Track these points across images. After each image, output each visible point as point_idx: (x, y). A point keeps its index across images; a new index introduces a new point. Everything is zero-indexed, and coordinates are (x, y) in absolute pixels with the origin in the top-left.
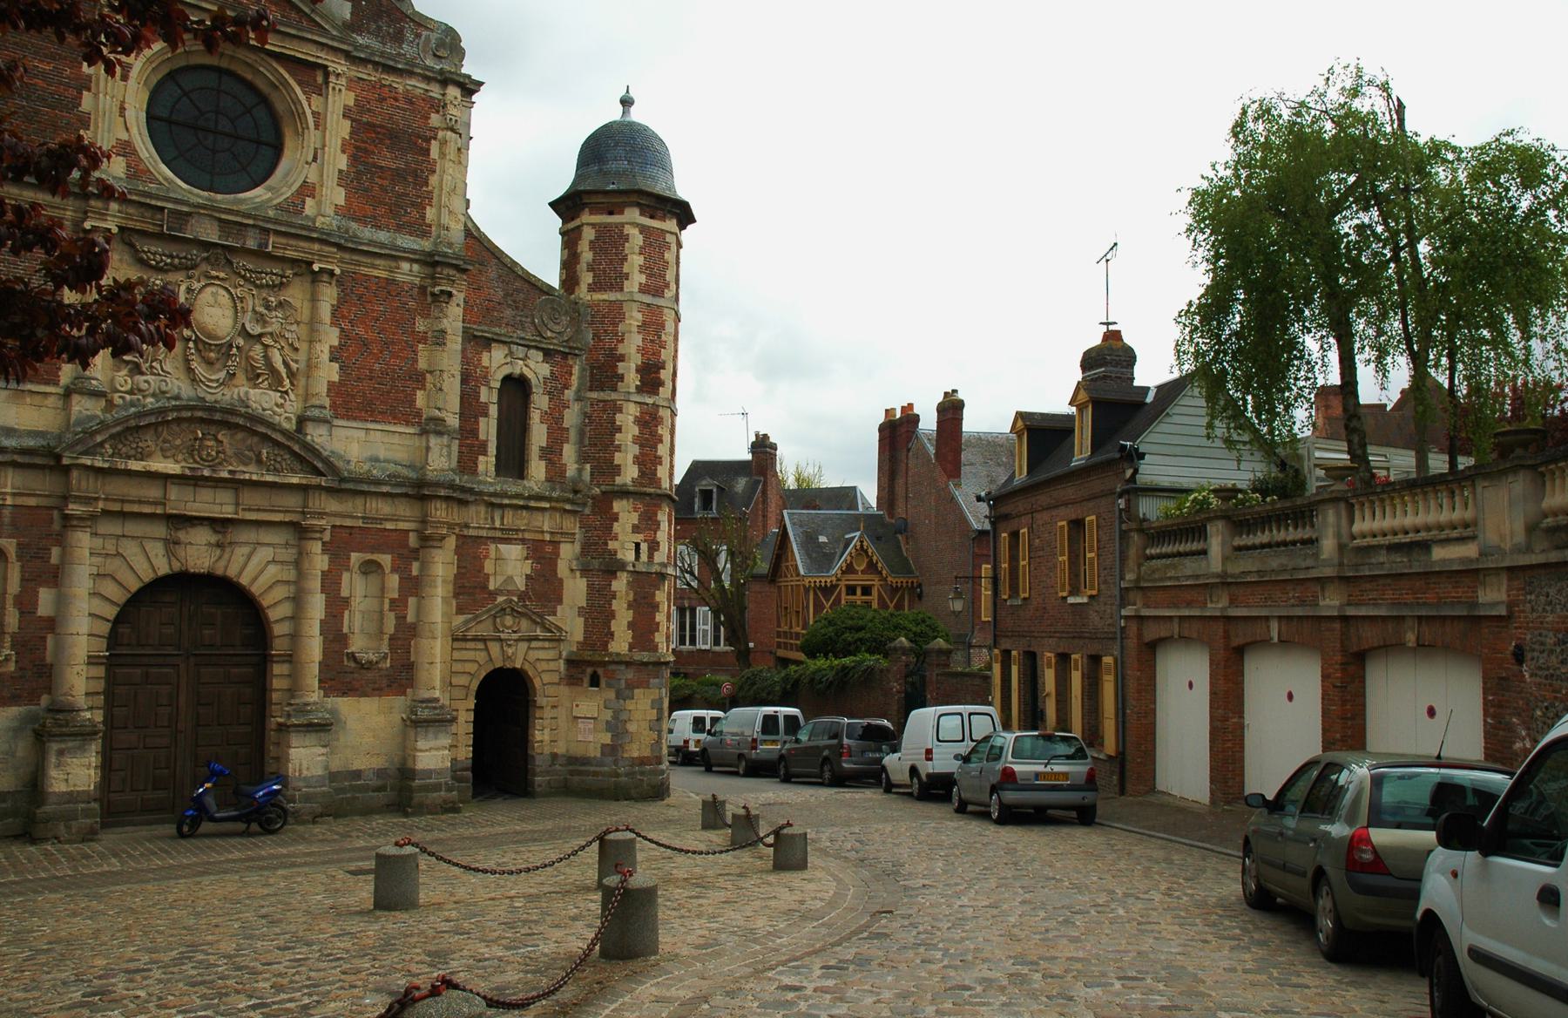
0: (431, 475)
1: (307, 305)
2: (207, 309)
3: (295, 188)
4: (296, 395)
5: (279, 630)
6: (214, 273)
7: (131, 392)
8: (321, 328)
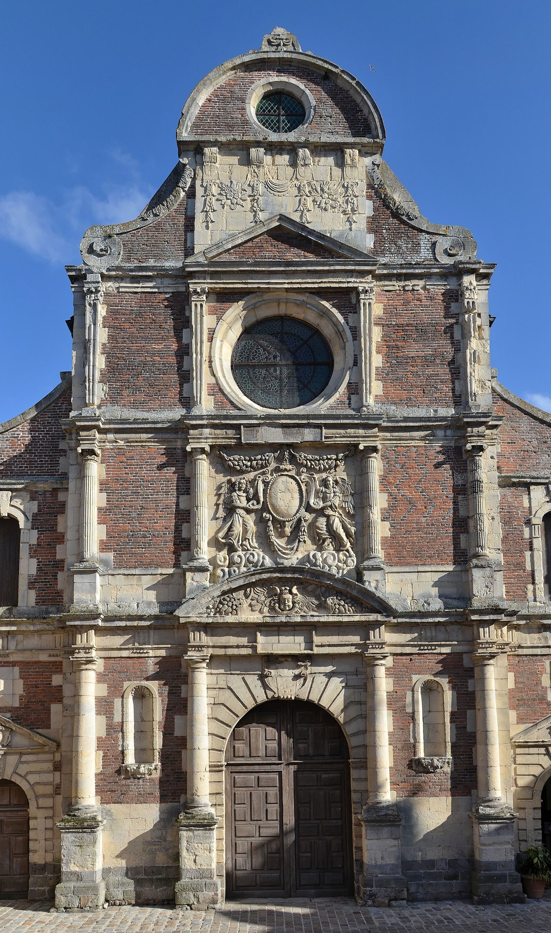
5: (352, 742)
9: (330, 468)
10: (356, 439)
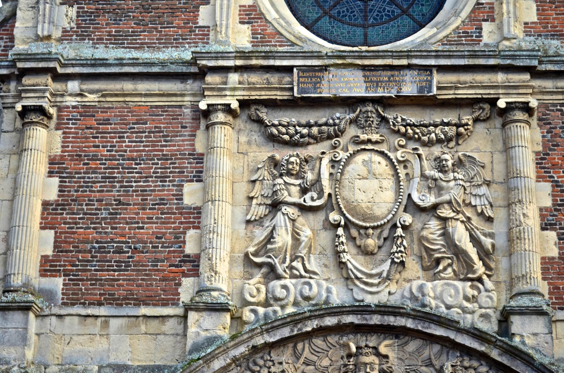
1: (499, 158)
2: (359, 183)
3: (464, 14)
4: (497, 283)
6: (364, 137)
7: (266, 304)
8: (520, 183)
9: (449, 140)
10: (492, 91)
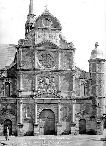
0: (72, 97)
